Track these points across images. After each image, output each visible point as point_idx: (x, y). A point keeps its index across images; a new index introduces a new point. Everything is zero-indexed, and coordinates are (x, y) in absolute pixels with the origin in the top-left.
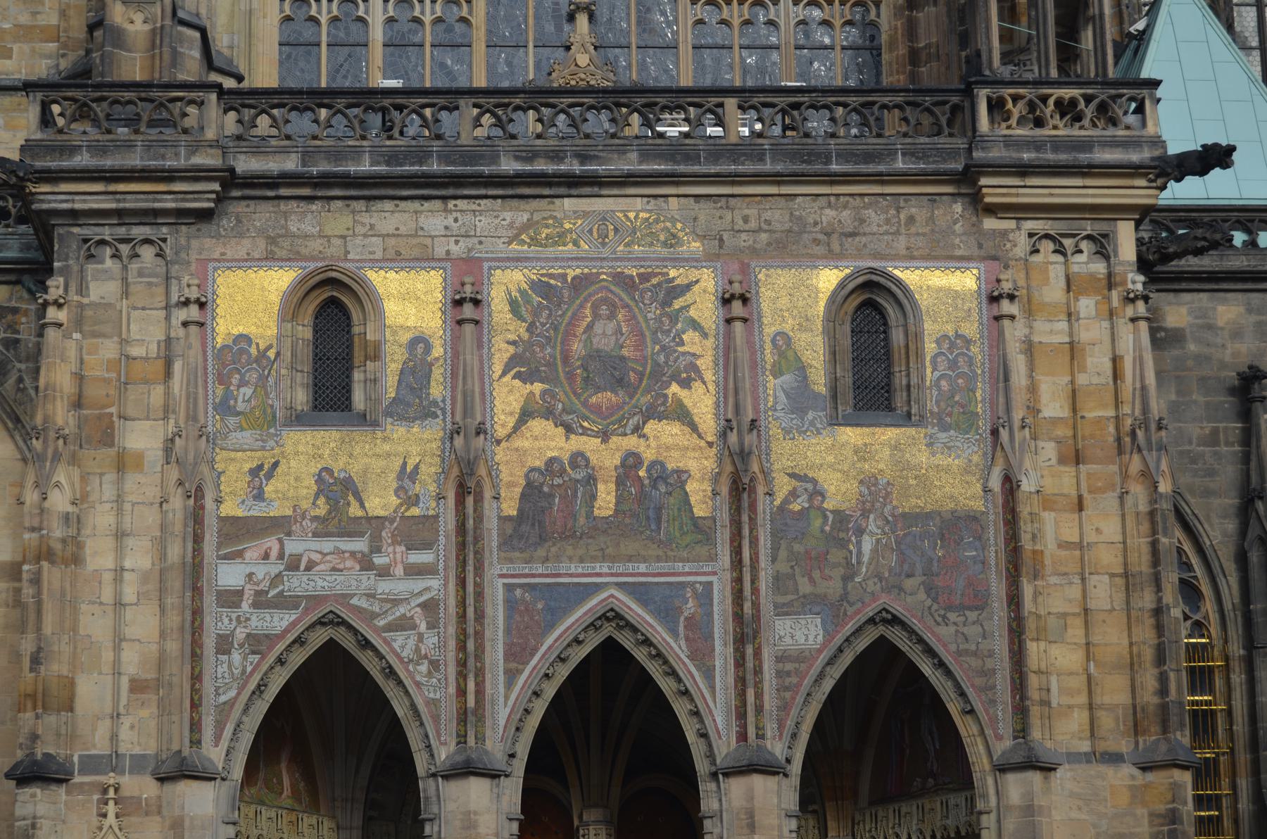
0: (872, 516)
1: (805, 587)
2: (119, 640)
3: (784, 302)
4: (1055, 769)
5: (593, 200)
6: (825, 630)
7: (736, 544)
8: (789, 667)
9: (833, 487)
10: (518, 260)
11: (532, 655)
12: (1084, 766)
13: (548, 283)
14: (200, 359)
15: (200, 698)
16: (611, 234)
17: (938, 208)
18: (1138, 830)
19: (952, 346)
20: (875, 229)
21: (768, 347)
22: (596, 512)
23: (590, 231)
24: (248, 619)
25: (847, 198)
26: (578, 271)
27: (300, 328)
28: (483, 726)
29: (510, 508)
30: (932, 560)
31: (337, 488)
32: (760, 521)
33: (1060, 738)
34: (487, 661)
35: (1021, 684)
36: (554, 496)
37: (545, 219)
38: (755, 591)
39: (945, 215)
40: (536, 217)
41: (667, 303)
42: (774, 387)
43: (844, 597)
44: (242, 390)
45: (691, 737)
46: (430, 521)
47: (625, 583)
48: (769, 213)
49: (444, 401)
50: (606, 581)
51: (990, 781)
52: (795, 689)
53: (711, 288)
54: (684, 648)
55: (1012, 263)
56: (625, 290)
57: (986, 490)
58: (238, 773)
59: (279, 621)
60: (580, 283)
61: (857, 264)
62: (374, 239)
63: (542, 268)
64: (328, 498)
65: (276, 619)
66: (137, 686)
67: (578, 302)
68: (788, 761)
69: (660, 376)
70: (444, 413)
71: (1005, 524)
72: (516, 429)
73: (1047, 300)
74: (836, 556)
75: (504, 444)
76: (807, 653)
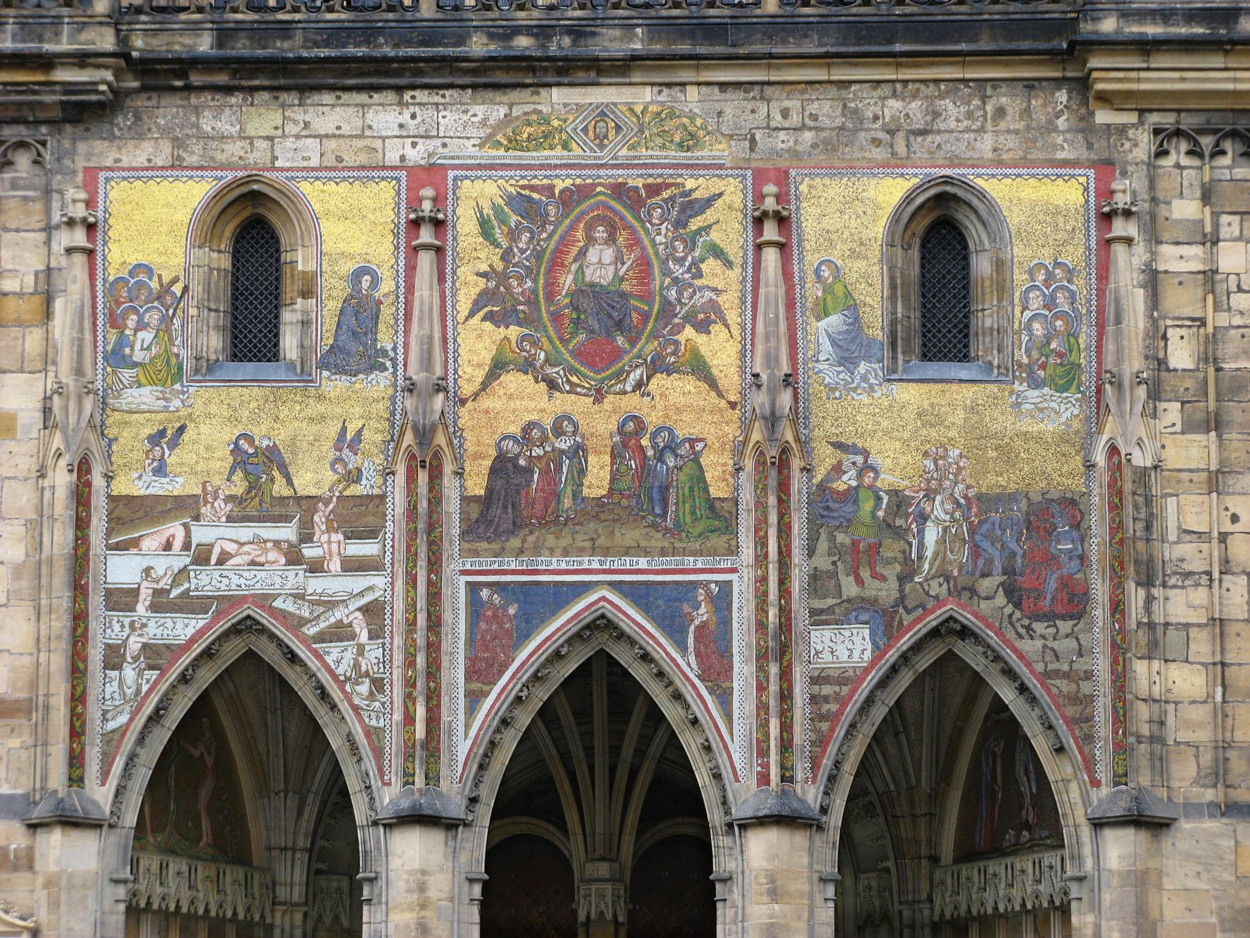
0: (938, 498)
1: (850, 588)
3: (833, 222)
4: (1168, 825)
5: (590, 89)
6: (874, 643)
7: (762, 533)
8: (827, 690)
9: (889, 461)
10: (492, 167)
13: (529, 199)
15: (84, 724)
16: (612, 133)
17: (1036, 97)
19: (1050, 277)
20: (953, 125)
23: (585, 130)
24: (144, 626)
25: (917, 85)
26: (569, 182)
27: (216, 255)
28: (437, 762)
29: (477, 486)
30: (1013, 554)
31: (257, 463)
32: (793, 505)
36: (532, 472)
37: (526, 114)
38: (784, 592)
39: (1045, 106)
40: (516, 111)
41: (680, 223)
42: (822, 331)
43: (901, 600)
44: (140, 335)
45: (703, 777)
49: (395, 349)
50: (596, 577)
52: (834, 718)
53: (738, 203)
54: (694, 665)
55: (1130, 169)
56: (631, 208)
58: (130, 819)
59: (183, 628)
60: (568, 199)
61: (928, 170)
62: (309, 141)
63: (523, 177)
64: (247, 474)
65: (179, 625)
67: (567, 222)
68: (824, 810)
70: (395, 366)
72: (485, 385)
74: (891, 549)
75: (469, 404)
76: (851, 673)
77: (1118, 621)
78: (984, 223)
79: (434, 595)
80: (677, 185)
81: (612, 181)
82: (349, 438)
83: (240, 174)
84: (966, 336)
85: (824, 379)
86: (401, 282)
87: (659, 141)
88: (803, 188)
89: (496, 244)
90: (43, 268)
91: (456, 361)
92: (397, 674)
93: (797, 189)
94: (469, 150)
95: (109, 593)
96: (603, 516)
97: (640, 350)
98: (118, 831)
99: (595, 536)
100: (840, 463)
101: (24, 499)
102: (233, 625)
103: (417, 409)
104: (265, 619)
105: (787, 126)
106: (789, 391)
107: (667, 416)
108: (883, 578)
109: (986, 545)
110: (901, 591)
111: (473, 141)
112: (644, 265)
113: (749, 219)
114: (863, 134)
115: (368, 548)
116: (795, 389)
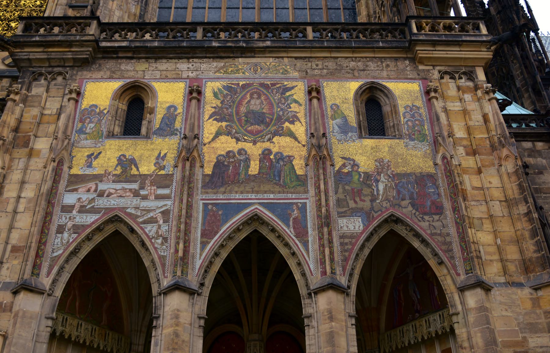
0: (382, 175)
2: (11, 228)
3: (335, 93)
5: (252, 59)
6: (363, 224)
7: (317, 185)
8: (346, 240)
10: (218, 78)
11: (215, 235)
12: (504, 288)
13: (231, 87)
14: (73, 112)
15: (44, 252)
16: (259, 70)
18: (540, 321)
20: (373, 69)
21: (329, 109)
22: (250, 173)
23: (250, 69)
24: (75, 218)
26: (244, 82)
28: (187, 268)
29: (208, 170)
30: (413, 193)
31: (126, 163)
33: (489, 276)
34: (192, 237)
35: (466, 247)
36: (229, 166)
38: (327, 205)
41: (283, 93)
42: (333, 125)
43: (372, 208)
44: (90, 125)
45: (297, 276)
46: (169, 177)
47: (263, 203)
49: (181, 129)
50: (254, 202)
51: (456, 297)
52: (351, 251)
53: (303, 88)
54: (293, 232)
57: (436, 164)
58: (58, 292)
60: (244, 87)
64: (122, 167)
65: (88, 218)
66: (15, 249)
67: (244, 93)
69: (280, 120)
71: (446, 178)
72: (213, 139)
73: (450, 95)
74: (366, 191)
75: (207, 145)
76: (355, 234)
77: (456, 214)
78: (386, 96)
79: (190, 206)
83: (132, 80)
84: (384, 131)
87: (275, 72)
89: (218, 99)
90: (59, 107)
92: (173, 235)
94: (211, 75)
95: (63, 207)
98: (52, 297)
100: (344, 164)
101: (38, 177)
102: (110, 218)
103: (187, 144)
104: (122, 215)
108: (364, 201)
109: (402, 190)
110: (372, 205)
112: (271, 105)
113: (307, 92)
115: (166, 191)
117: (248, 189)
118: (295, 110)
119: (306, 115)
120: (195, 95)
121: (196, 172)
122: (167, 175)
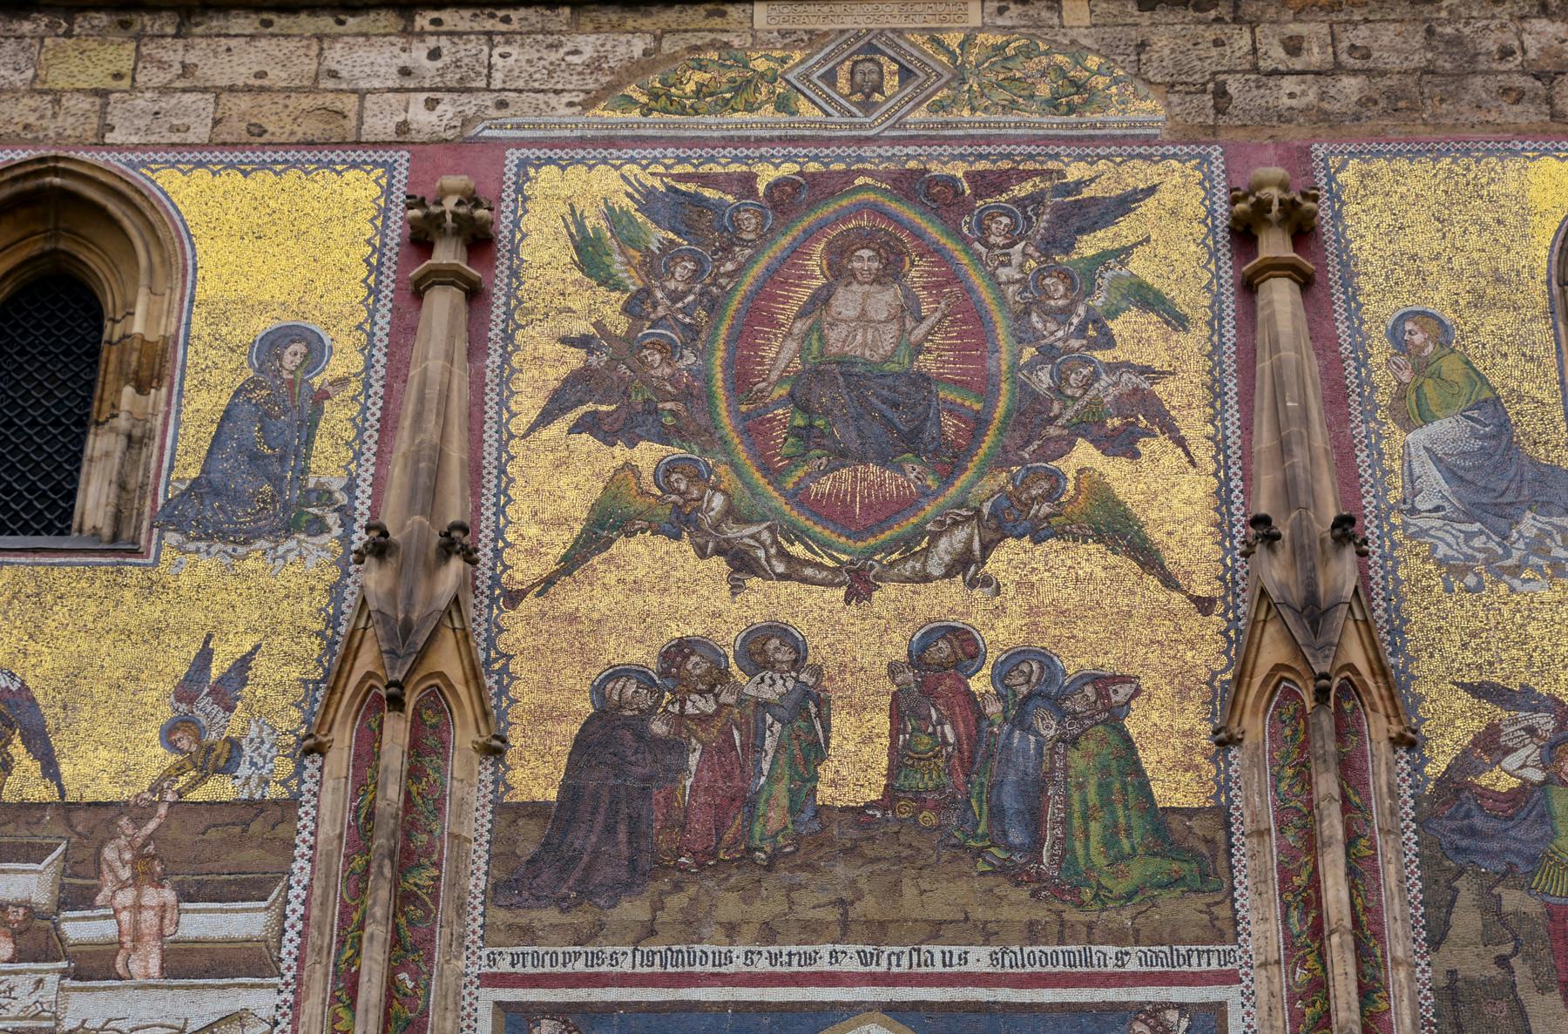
3: (1423, 239)
10: (610, 142)
13: (697, 201)
16: (891, 83)
21: (1380, 350)
22: (824, 793)
23: (830, 78)
26: (788, 169)
29: (537, 776)
36: (682, 749)
37: (697, 48)
41: (1058, 241)
42: (1411, 459)
46: (271, 817)
47: (916, 1006)
48: (1363, 31)
49: (350, 488)
53: (1193, 201)
60: (786, 199)
62: (188, 98)
63: (680, 160)
67: (785, 241)
72: (572, 562)
75: (530, 604)
80: (1045, 174)
81: (892, 167)
82: (215, 672)
83: (21, 155)
85: (1434, 548)
86: (378, 355)
87: (1002, 96)
88: (1348, 177)
89: (610, 282)
91: (500, 511)
93: (1331, 179)
94: (562, 115)
96: (868, 850)
97: (966, 490)
99: (847, 895)
100: (1493, 731)
103: (392, 594)
105: (1298, 67)
106: (1349, 553)
107: (1033, 627)
111: (566, 98)
112: (972, 323)
113: (1222, 234)
114: (1479, 80)
115: (241, 922)
116: (1363, 554)
117: (810, 905)
118: (1143, 357)
119: (1216, 391)
120: (447, 254)
121: (455, 788)
122: (255, 806)
